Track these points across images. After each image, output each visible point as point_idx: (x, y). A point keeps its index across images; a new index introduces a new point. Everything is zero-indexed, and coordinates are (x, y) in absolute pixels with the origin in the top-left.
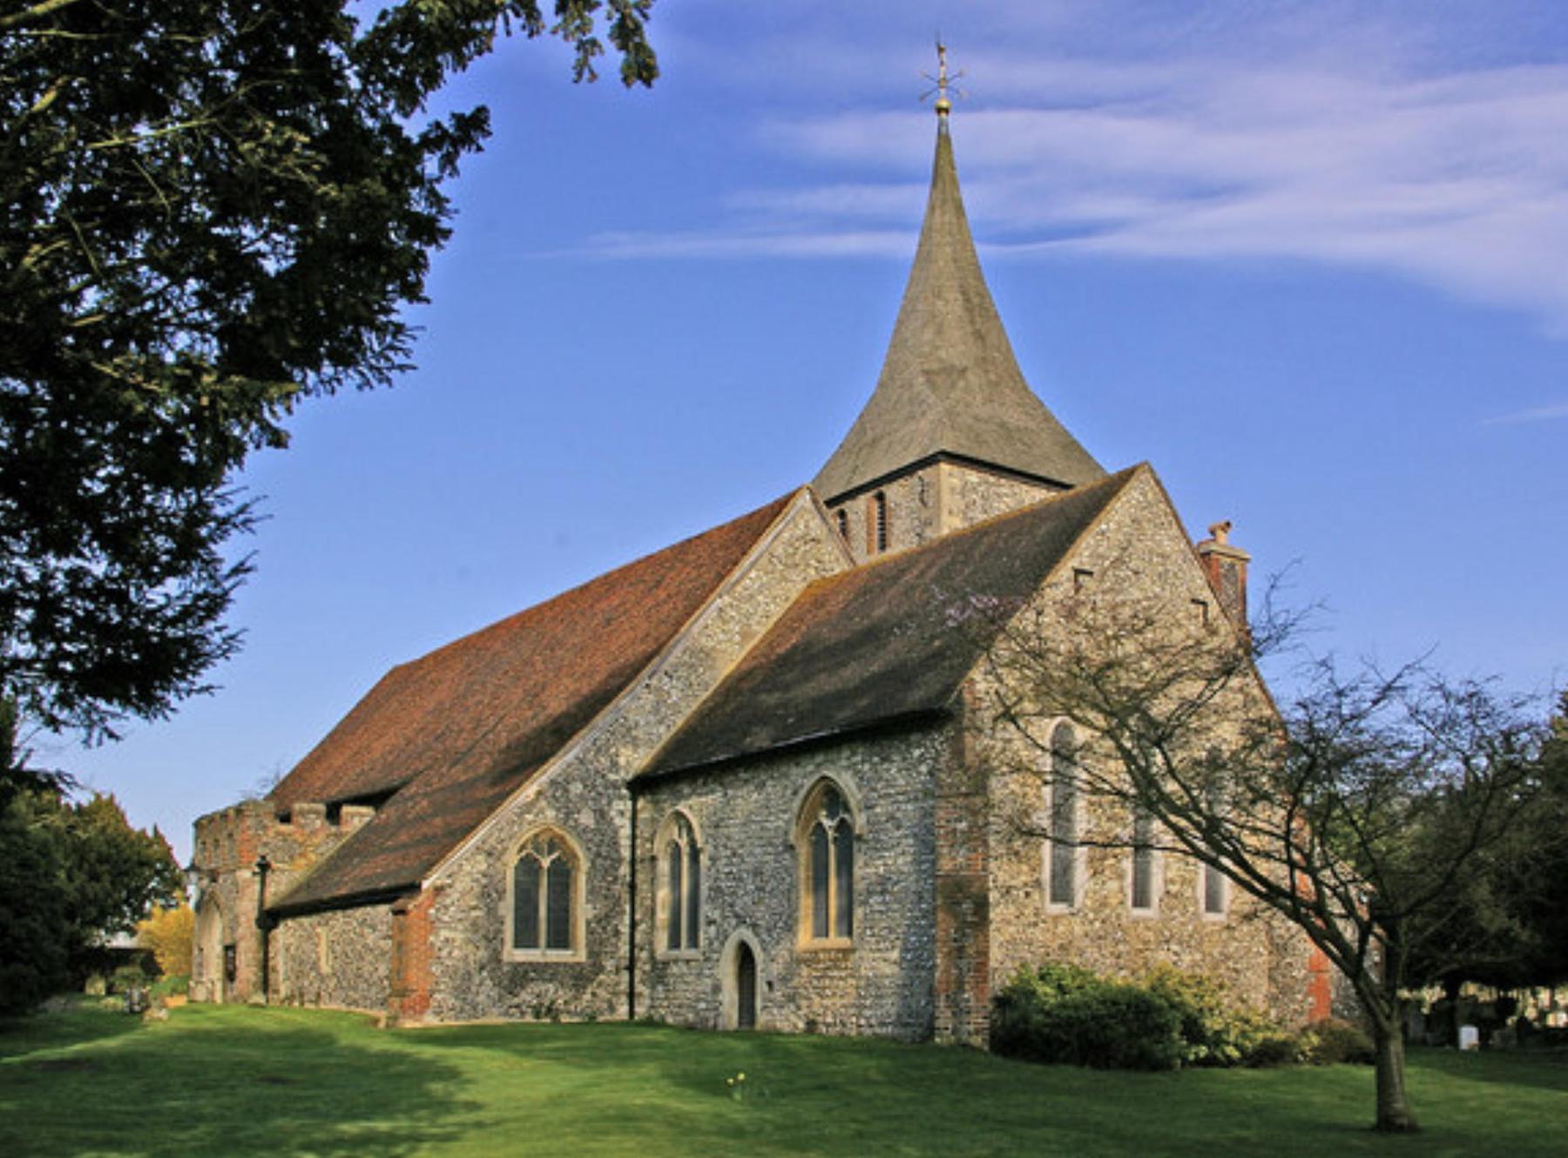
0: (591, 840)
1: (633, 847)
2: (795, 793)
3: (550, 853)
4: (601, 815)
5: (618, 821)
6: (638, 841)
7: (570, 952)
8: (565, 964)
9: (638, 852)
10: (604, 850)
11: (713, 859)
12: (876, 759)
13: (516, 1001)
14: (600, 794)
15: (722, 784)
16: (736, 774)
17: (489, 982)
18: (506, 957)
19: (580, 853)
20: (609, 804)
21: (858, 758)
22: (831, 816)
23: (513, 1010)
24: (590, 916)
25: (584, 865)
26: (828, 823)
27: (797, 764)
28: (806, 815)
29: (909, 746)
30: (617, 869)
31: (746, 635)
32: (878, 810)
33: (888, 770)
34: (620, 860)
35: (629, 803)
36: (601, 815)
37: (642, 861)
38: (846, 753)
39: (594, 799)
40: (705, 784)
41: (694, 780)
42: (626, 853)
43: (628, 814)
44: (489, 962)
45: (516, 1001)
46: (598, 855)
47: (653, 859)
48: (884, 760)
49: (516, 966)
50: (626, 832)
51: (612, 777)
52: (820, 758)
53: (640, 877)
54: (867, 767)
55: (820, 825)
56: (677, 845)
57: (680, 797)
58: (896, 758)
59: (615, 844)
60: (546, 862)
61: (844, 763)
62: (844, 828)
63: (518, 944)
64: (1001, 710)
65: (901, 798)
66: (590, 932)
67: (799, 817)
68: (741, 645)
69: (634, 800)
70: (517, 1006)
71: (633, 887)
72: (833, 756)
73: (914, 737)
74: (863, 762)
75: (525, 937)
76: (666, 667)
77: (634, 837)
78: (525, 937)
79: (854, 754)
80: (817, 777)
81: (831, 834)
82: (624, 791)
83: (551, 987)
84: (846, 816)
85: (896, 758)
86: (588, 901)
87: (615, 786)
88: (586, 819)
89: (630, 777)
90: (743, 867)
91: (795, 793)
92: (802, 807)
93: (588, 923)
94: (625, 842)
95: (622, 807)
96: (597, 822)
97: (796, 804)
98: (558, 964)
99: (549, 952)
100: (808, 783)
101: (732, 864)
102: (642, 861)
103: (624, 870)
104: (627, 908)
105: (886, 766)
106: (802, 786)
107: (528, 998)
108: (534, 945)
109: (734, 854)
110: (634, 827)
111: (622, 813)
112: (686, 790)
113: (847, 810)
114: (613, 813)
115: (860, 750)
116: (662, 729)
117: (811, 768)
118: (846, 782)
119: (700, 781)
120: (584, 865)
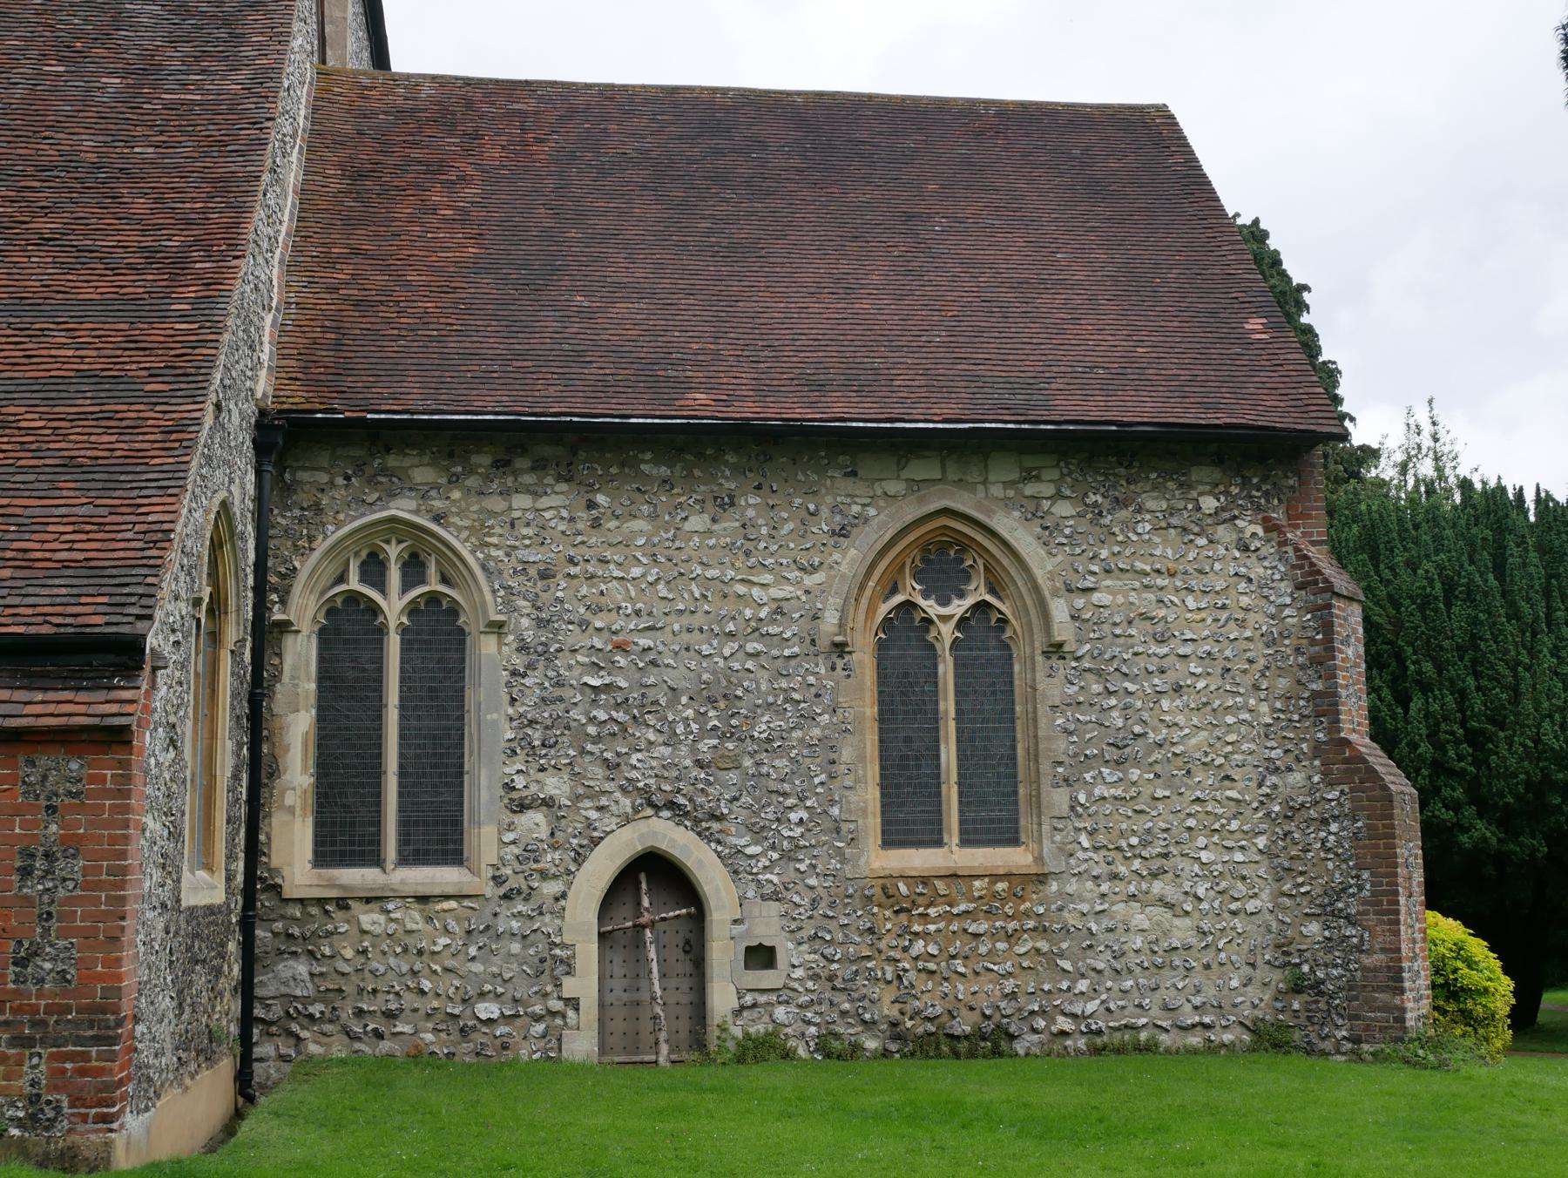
16: (634, 464)
26: (931, 607)
32: (1096, 597)
33: (1130, 526)
40: (502, 465)
48: (1120, 503)
54: (1064, 509)
57: (395, 485)
61: (997, 491)
65: (1160, 582)
72: (974, 476)
74: (1058, 496)
79: (1030, 476)
90: (671, 677)
91: (842, 533)
101: (613, 667)
105: (1124, 514)
112: (423, 475)
115: (1055, 475)
117: (894, 487)
119: (483, 460)
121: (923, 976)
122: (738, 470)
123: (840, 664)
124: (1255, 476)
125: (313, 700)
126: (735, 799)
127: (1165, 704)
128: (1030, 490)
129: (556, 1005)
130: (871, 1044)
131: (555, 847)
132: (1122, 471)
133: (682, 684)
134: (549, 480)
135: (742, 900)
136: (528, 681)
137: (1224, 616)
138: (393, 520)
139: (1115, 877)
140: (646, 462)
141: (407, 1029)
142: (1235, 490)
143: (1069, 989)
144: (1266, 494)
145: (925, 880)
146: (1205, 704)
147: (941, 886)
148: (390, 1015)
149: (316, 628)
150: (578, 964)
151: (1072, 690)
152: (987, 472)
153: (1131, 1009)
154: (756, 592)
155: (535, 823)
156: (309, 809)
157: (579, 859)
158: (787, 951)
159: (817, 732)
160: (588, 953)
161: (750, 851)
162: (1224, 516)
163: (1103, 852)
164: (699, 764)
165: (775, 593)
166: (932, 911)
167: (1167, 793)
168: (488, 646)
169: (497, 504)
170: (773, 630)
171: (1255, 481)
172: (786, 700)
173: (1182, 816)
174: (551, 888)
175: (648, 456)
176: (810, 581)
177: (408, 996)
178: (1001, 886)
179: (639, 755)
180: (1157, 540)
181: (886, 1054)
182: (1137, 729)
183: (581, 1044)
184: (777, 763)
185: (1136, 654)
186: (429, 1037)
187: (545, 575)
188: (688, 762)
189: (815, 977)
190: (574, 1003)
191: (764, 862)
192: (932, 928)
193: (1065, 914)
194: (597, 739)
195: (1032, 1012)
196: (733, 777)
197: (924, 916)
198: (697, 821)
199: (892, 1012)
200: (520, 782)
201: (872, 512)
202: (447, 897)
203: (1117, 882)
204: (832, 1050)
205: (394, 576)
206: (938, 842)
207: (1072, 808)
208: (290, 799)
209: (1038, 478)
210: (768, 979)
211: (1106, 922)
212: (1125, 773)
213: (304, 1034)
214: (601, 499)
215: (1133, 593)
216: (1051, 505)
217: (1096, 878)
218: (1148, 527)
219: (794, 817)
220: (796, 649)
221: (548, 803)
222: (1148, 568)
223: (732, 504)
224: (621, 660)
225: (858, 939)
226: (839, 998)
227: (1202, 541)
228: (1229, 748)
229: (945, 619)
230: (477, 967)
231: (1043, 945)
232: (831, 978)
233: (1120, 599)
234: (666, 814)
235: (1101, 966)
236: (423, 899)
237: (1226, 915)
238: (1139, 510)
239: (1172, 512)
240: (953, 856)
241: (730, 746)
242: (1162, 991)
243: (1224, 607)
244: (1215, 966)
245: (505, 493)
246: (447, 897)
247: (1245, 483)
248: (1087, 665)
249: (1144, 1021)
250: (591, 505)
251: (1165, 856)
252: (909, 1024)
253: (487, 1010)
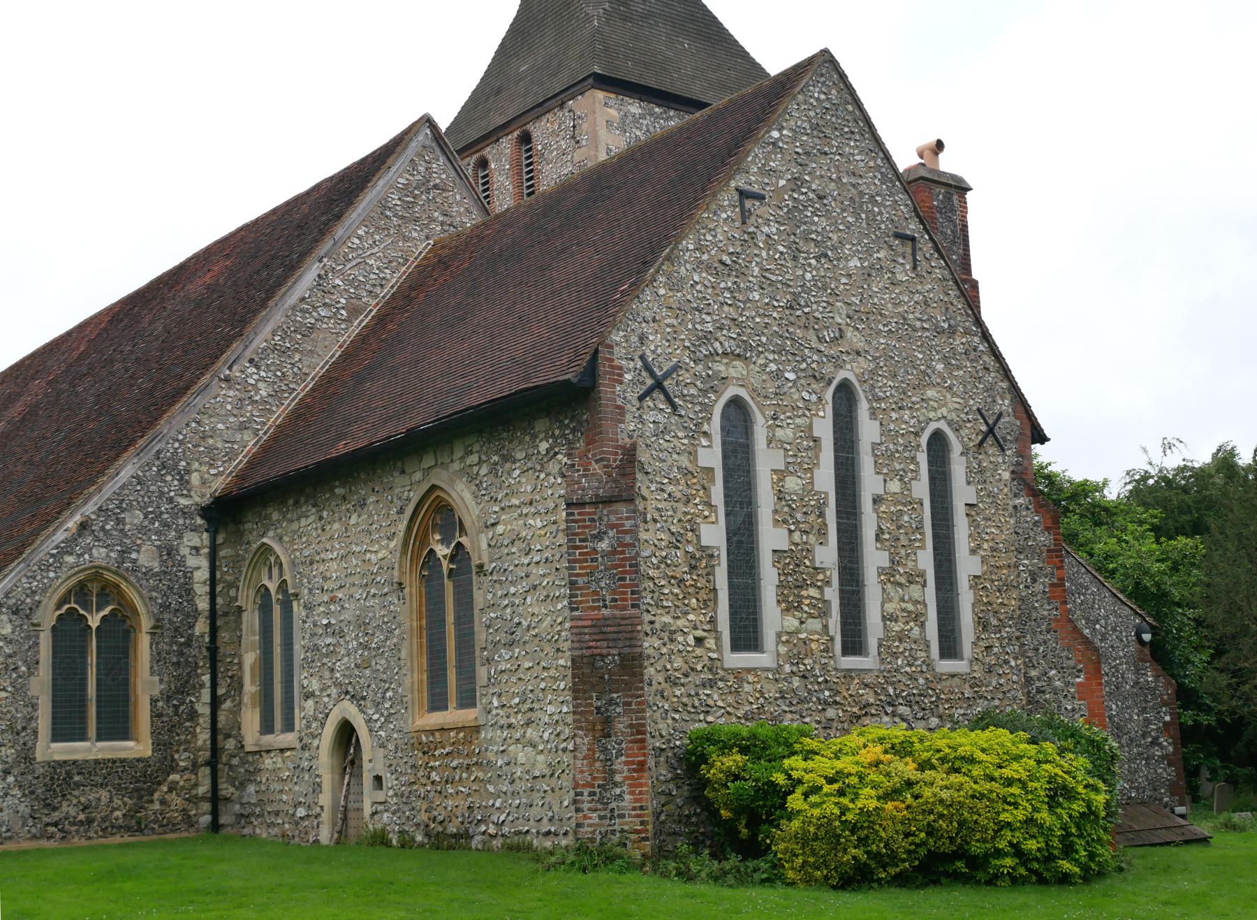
0: (154, 589)
1: (213, 595)
2: (401, 511)
3: (98, 610)
4: (169, 552)
5: (192, 562)
6: (219, 588)
7: (130, 744)
8: (123, 761)
9: (219, 600)
10: (173, 601)
11: (309, 607)
12: (496, 458)
13: (56, 816)
14: (166, 525)
15: (315, 505)
16: (332, 490)
17: (16, 792)
18: (40, 755)
19: (141, 609)
20: (180, 537)
21: (474, 458)
22: (445, 541)
23: (51, 829)
24: (156, 692)
25: (146, 623)
26: (442, 551)
27: (403, 472)
28: (415, 541)
29: (534, 437)
30: (192, 627)
31: (354, 312)
32: (500, 529)
34: (196, 613)
35: (205, 535)
36: (169, 552)
37: (226, 614)
38: (458, 454)
39: (158, 533)
40: (297, 503)
41: (284, 502)
42: (203, 605)
43: (206, 550)
44: (17, 763)
45: (56, 816)
46: (165, 607)
47: (240, 610)
49: (55, 766)
50: (202, 575)
51: (183, 502)
52: (428, 461)
53: (224, 636)
55: (432, 551)
56: (267, 589)
58: (520, 455)
59: (189, 591)
60: (94, 621)
61: (456, 466)
62: (459, 553)
63: (57, 736)
64: (649, 382)
66: (156, 715)
67: (405, 543)
68: (348, 320)
69: (213, 529)
70: (55, 825)
71: (213, 650)
72: (447, 460)
73: (541, 425)
74: (480, 463)
75: (66, 728)
76: (248, 354)
77: (213, 582)
78: (66, 728)
80: (426, 487)
81: (445, 564)
82: (199, 521)
83: (104, 794)
84: (463, 540)
85: (520, 455)
86: (152, 674)
87: (184, 513)
88: (146, 557)
89: (206, 500)
90: (346, 616)
91: (401, 511)
92: (409, 529)
93: (154, 702)
94: (201, 590)
95: (196, 541)
96: (163, 562)
97: (402, 526)
98: (114, 762)
99: (100, 744)
100: (415, 497)
102: (226, 614)
103: (201, 627)
104: (206, 678)
105: (508, 465)
106: (409, 499)
107: (72, 811)
108: (82, 737)
109: (333, 600)
110: (213, 569)
111: (197, 549)
112: (275, 516)
113: (463, 530)
114: (184, 551)
116: (247, 436)
117: (418, 476)
118: (462, 495)
119: (291, 502)
120: (146, 623)
121: (437, 795)
122: (365, 482)
123: (401, 594)
124: (566, 418)
125: (257, 645)
126: (369, 686)
127: (529, 600)
128: (468, 462)
129: (318, 810)
130: (419, 838)
131: (316, 719)
132: (505, 435)
133: (351, 619)
134: (310, 508)
135: (373, 747)
136: (306, 626)
137: (555, 527)
138: (264, 544)
139: (510, 726)
140: (336, 487)
141: (280, 821)
142: (557, 432)
143: (493, 805)
144: (574, 431)
145: (432, 732)
146: (548, 596)
147: (437, 734)
148: (277, 814)
149: (257, 606)
150: (323, 785)
151: (490, 596)
152: (452, 453)
153: (521, 820)
154: (373, 557)
155: (310, 703)
156: (257, 704)
157: (323, 725)
158: (389, 780)
159: (395, 640)
160: (327, 780)
161: (376, 717)
162: (551, 454)
163: (505, 709)
164: (357, 666)
165: (380, 556)
166: (437, 753)
167: (531, 665)
168: (295, 604)
169: (295, 526)
170: (378, 579)
171: (566, 422)
172: (384, 622)
173: (539, 680)
174: (316, 743)
175: (337, 483)
176: (392, 544)
177: (281, 804)
178: (461, 735)
179: (338, 664)
180: (524, 480)
181: (422, 845)
182: (516, 620)
183: (325, 835)
184: (383, 662)
185: (516, 566)
186: (287, 826)
187: (311, 563)
188: (353, 666)
189: (396, 795)
190: (322, 807)
191: (379, 724)
192: (437, 763)
193: (488, 753)
194: (327, 656)
195: (479, 821)
196: (367, 672)
197: (434, 755)
198: (358, 701)
199: (424, 817)
200: (305, 682)
201: (412, 494)
202: (288, 749)
203: (511, 730)
204: (406, 843)
205: (275, 572)
206: (446, 708)
207: (489, 679)
208: (246, 699)
209: (471, 452)
210: (380, 796)
211: (506, 759)
212: (514, 653)
213: (255, 823)
214: (325, 514)
215: (515, 523)
216: (479, 469)
217: (502, 727)
218: (518, 472)
219: (389, 694)
220: (386, 590)
221: (312, 694)
222: (517, 502)
223: (365, 504)
224: (332, 607)
225: (409, 771)
226: (406, 808)
227: (542, 476)
228: (559, 628)
229: (445, 557)
230: (297, 788)
231: (481, 775)
232: (402, 795)
233: (509, 527)
234: (348, 697)
235: (504, 789)
236: (282, 751)
237: (560, 752)
238: (514, 462)
239: (528, 457)
240: (453, 716)
241: (366, 653)
242: (534, 807)
243: (555, 522)
244: (557, 790)
245: (299, 519)
246: (288, 749)
247: (563, 427)
248: (495, 578)
249: (526, 828)
250: (321, 518)
251: (531, 710)
252: (433, 826)
253: (301, 812)
